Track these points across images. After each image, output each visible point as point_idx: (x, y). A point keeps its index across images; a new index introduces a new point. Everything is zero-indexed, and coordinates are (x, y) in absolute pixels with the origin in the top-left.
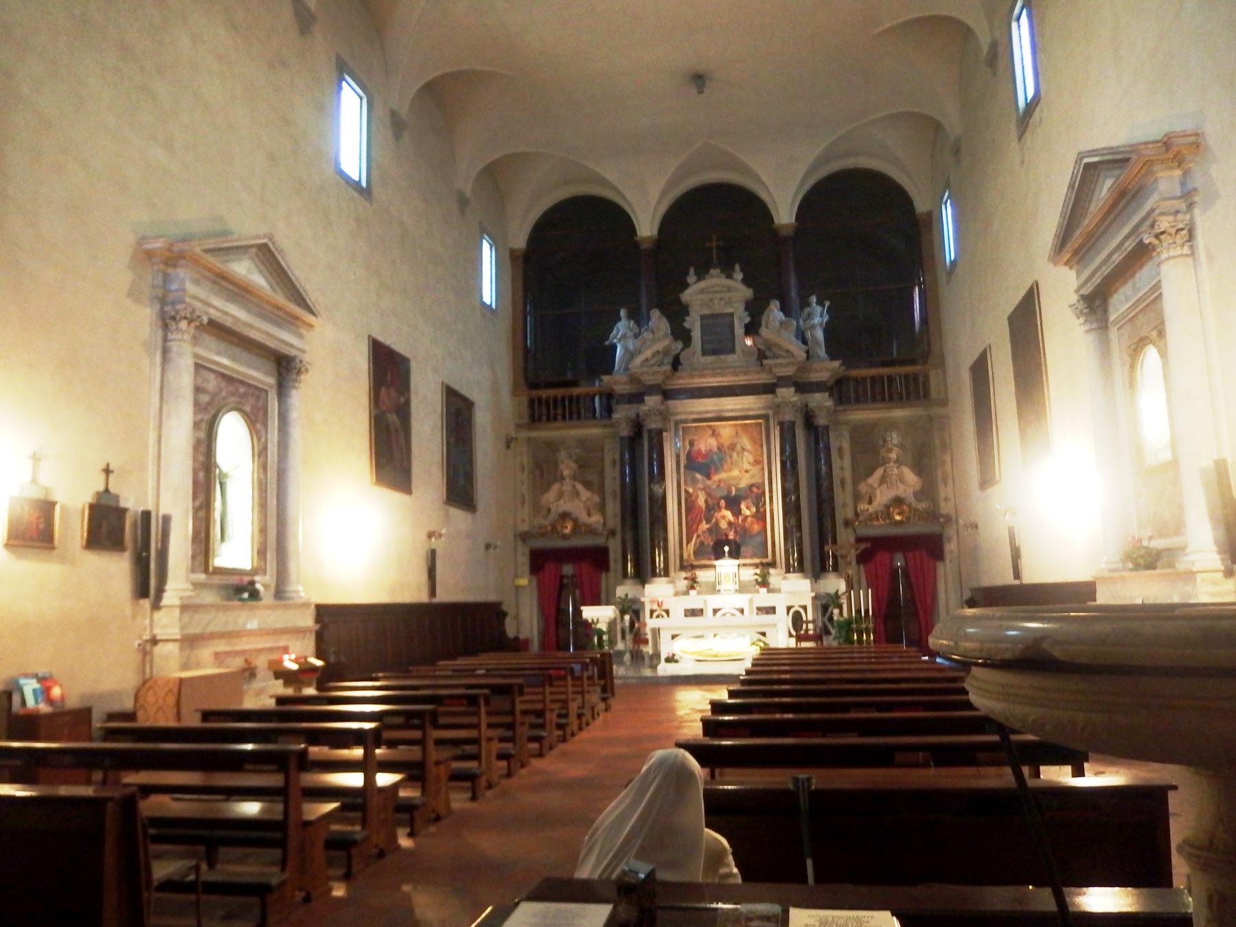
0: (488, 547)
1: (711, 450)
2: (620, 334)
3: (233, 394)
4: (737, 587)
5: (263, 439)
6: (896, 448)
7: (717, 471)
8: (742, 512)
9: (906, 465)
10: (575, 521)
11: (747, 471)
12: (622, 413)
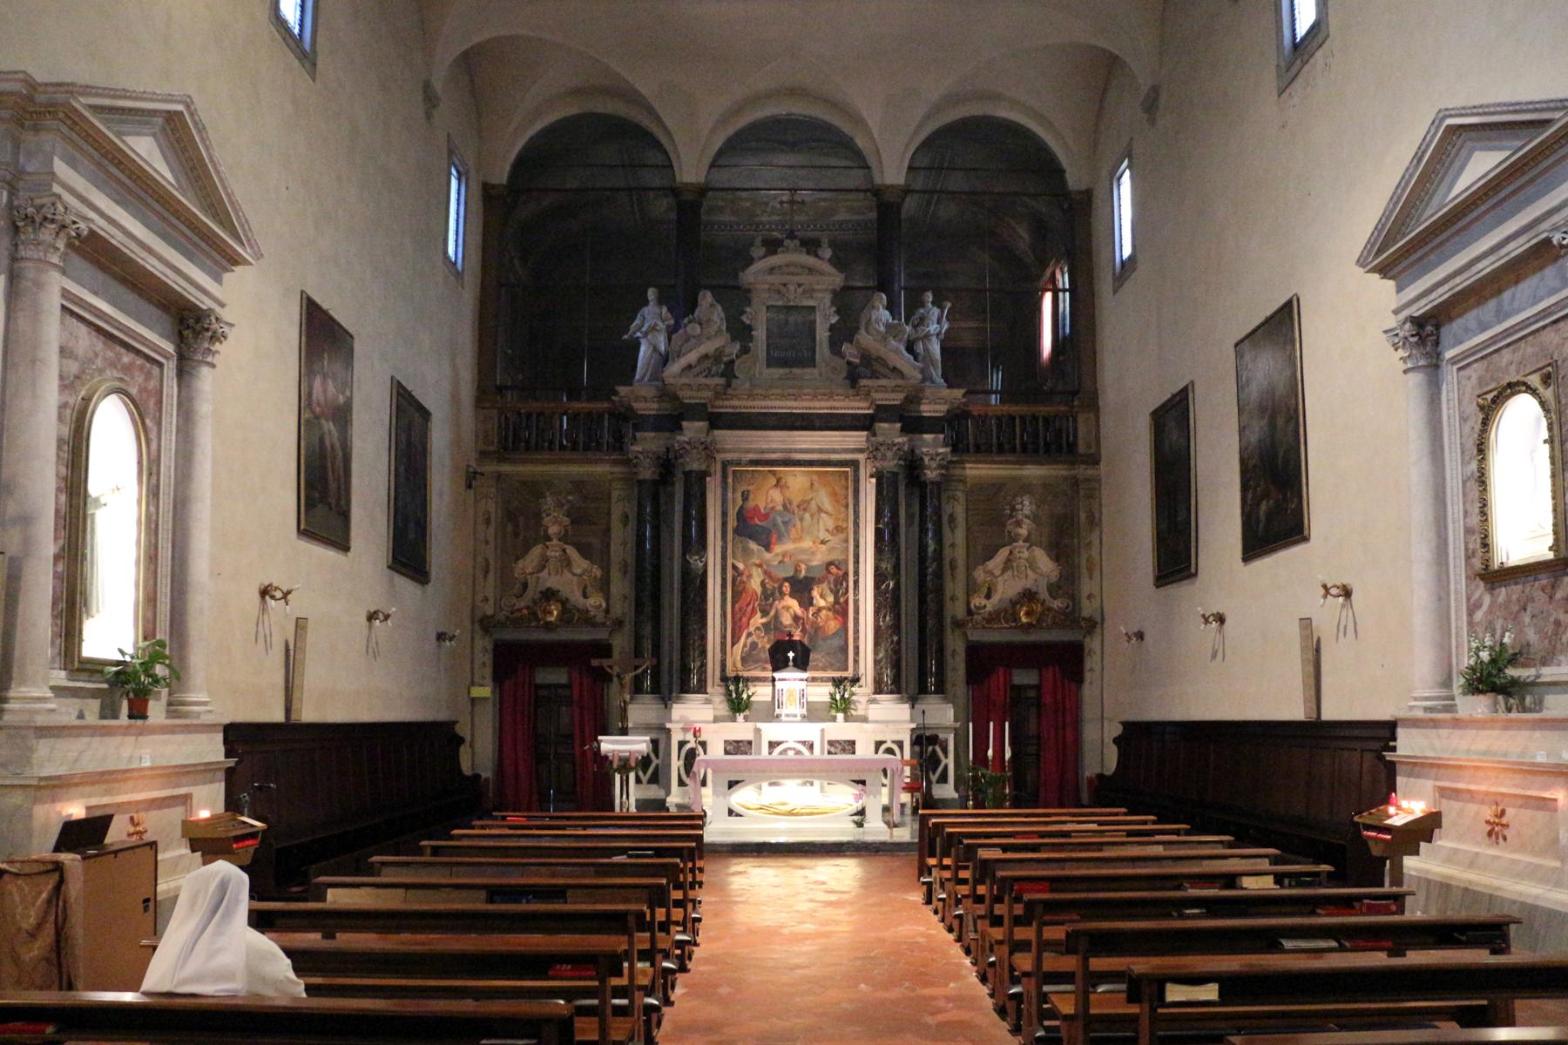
0: (441, 637)
1: (773, 508)
2: (646, 326)
3: (113, 365)
4: (804, 711)
5: (154, 446)
6: (1027, 521)
7: (780, 538)
8: (815, 602)
9: (1040, 545)
10: (564, 603)
11: (823, 542)
12: (647, 444)
